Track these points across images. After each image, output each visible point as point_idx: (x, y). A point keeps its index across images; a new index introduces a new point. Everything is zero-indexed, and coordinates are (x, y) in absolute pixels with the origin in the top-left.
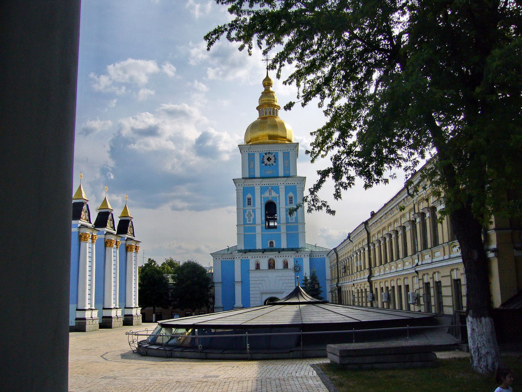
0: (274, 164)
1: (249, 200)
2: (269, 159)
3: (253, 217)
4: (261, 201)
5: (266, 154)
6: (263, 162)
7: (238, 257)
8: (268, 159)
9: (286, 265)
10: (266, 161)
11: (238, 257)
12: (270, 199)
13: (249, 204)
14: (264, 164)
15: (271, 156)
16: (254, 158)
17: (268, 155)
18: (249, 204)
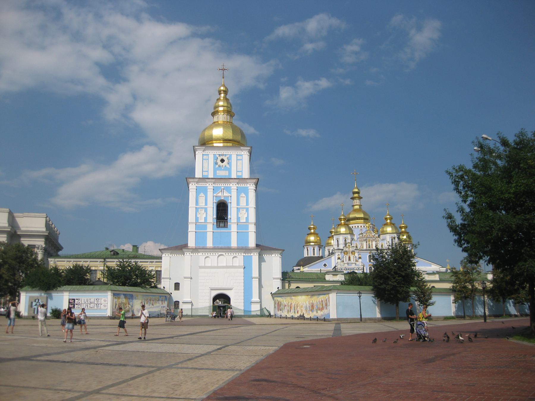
0: (228, 166)
5: (219, 155)
6: (216, 163)
10: (220, 163)
12: (222, 198)
15: (225, 158)
16: (208, 159)
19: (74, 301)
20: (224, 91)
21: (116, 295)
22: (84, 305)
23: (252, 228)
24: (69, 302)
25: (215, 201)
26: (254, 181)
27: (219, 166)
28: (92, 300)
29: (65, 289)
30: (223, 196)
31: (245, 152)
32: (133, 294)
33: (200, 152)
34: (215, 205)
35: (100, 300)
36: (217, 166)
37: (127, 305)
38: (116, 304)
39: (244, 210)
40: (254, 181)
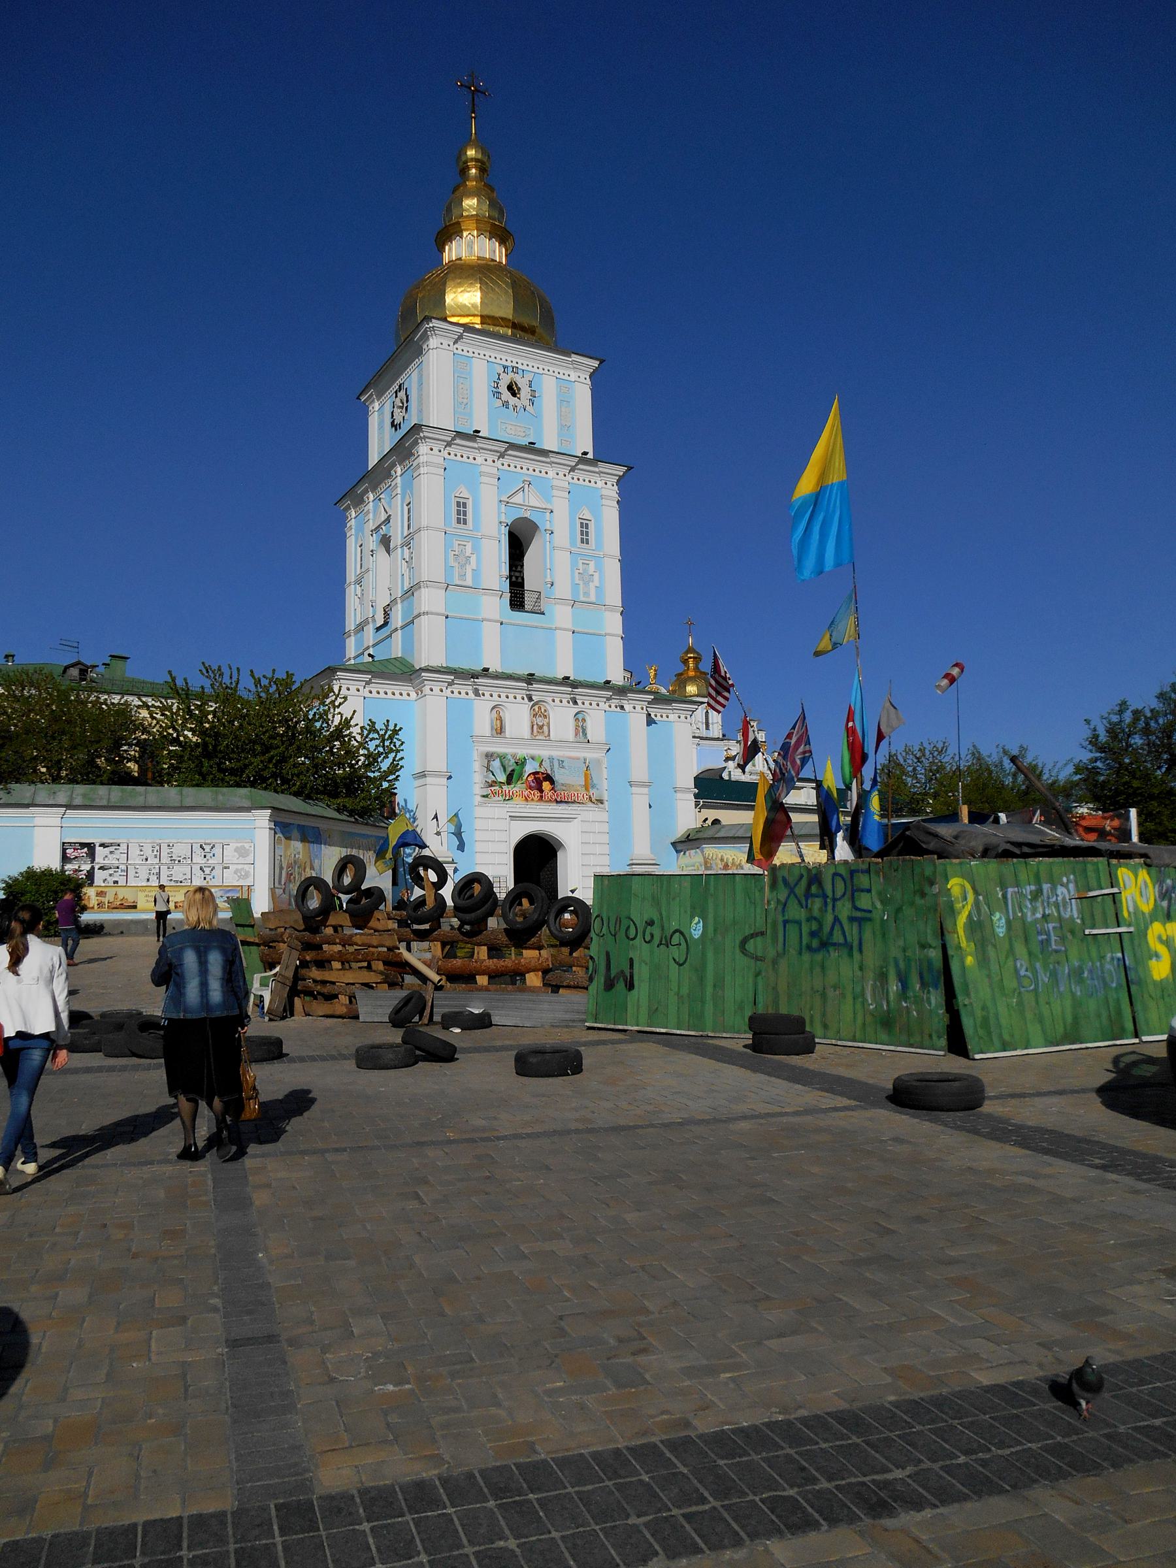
1: (461, 506)
2: (513, 389)
3: (473, 564)
4: (499, 513)
5: (505, 367)
7: (436, 689)
8: (510, 388)
9: (581, 729)
10: (506, 395)
11: (436, 689)
12: (527, 515)
13: (462, 519)
14: (499, 403)
15: (522, 383)
17: (511, 375)
18: (462, 519)
19: (92, 855)
20: (477, 160)
21: (283, 826)
22: (143, 874)
23: (614, 623)
24: (65, 859)
25: (503, 519)
26: (620, 470)
27: (506, 404)
28: (181, 850)
29: (38, 800)
30: (529, 503)
31: (583, 376)
32: (322, 825)
33: (445, 342)
34: (505, 531)
35: (217, 850)
36: (499, 403)
37: (308, 869)
38: (281, 868)
39: (585, 563)
40: (620, 470)
